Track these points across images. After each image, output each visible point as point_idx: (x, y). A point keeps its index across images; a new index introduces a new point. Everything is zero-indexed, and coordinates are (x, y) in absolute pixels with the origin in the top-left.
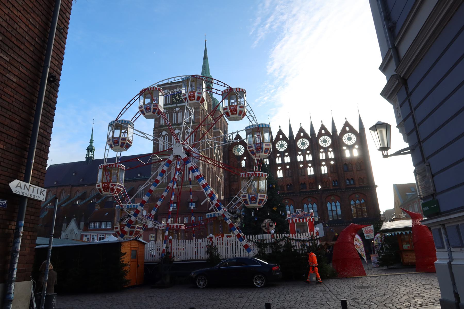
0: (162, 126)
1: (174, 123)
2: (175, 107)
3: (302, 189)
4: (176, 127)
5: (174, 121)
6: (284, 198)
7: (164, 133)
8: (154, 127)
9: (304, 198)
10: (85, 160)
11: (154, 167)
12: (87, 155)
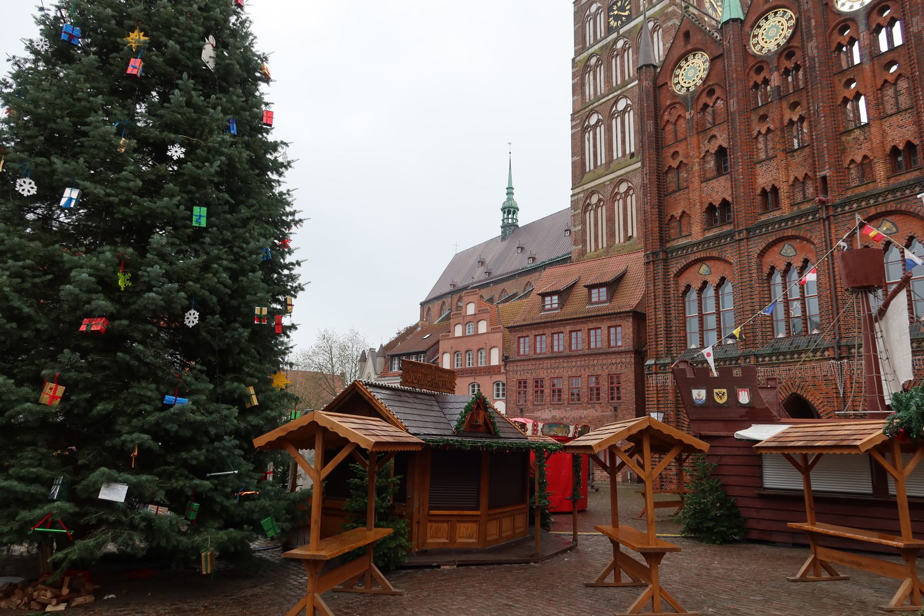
2: (615, 41)
4: (619, 92)
5: (617, 79)
7: (593, 120)
10: (498, 232)
11: (576, 212)
12: (503, 220)
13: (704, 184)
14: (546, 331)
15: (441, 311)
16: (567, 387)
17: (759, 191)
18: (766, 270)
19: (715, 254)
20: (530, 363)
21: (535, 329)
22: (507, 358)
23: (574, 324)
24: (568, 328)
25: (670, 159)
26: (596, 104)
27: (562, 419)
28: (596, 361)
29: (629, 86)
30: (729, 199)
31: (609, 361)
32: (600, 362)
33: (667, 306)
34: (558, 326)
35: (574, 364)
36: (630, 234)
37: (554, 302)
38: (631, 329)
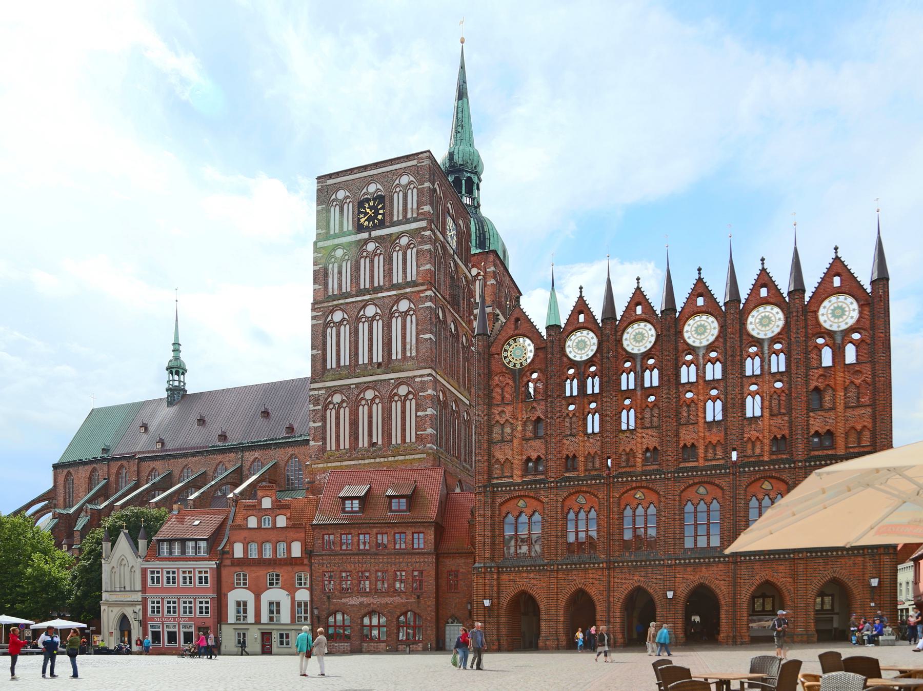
0: (335, 297)
1: (362, 287)
3: (685, 460)
5: (365, 283)
6: (634, 485)
7: (338, 316)
8: (312, 301)
9: (688, 487)
13: (524, 442)
14: (353, 531)
15: (90, 478)
17: (564, 456)
18: (566, 510)
19: (532, 494)
21: (341, 529)
22: (311, 552)
23: (380, 527)
24: (375, 530)
25: (497, 416)
26: (342, 301)
29: (380, 295)
30: (542, 456)
32: (405, 560)
33: (493, 525)
34: (366, 528)
36: (374, 440)
38: (433, 536)
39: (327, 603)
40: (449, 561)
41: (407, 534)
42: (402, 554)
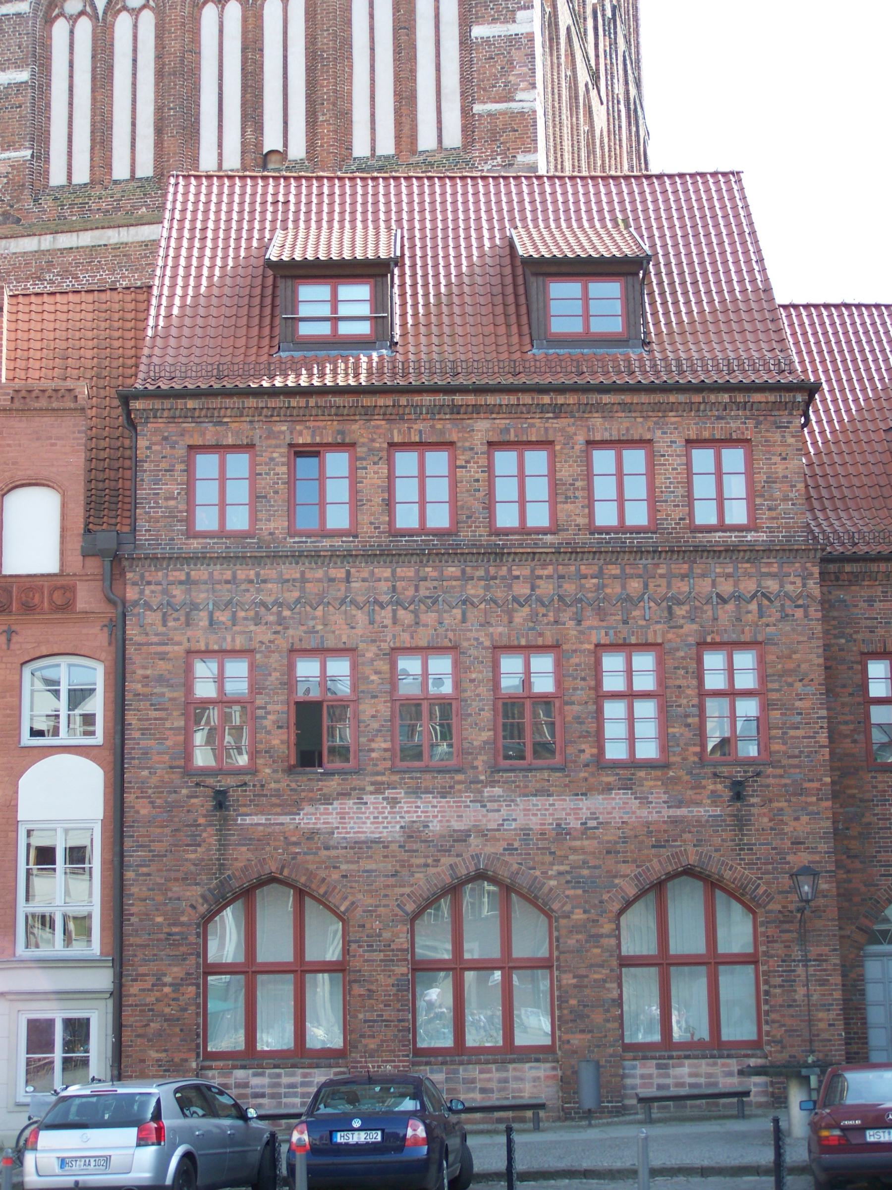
16: (484, 691)
20: (268, 572)
23: (512, 411)
27: (462, 837)
28: (635, 585)
31: (704, 586)
32: (659, 587)
34: (435, 411)
35: (522, 589)
37: (344, 310)
39: (210, 836)
40: (870, 601)
41: (661, 446)
42: (640, 552)
